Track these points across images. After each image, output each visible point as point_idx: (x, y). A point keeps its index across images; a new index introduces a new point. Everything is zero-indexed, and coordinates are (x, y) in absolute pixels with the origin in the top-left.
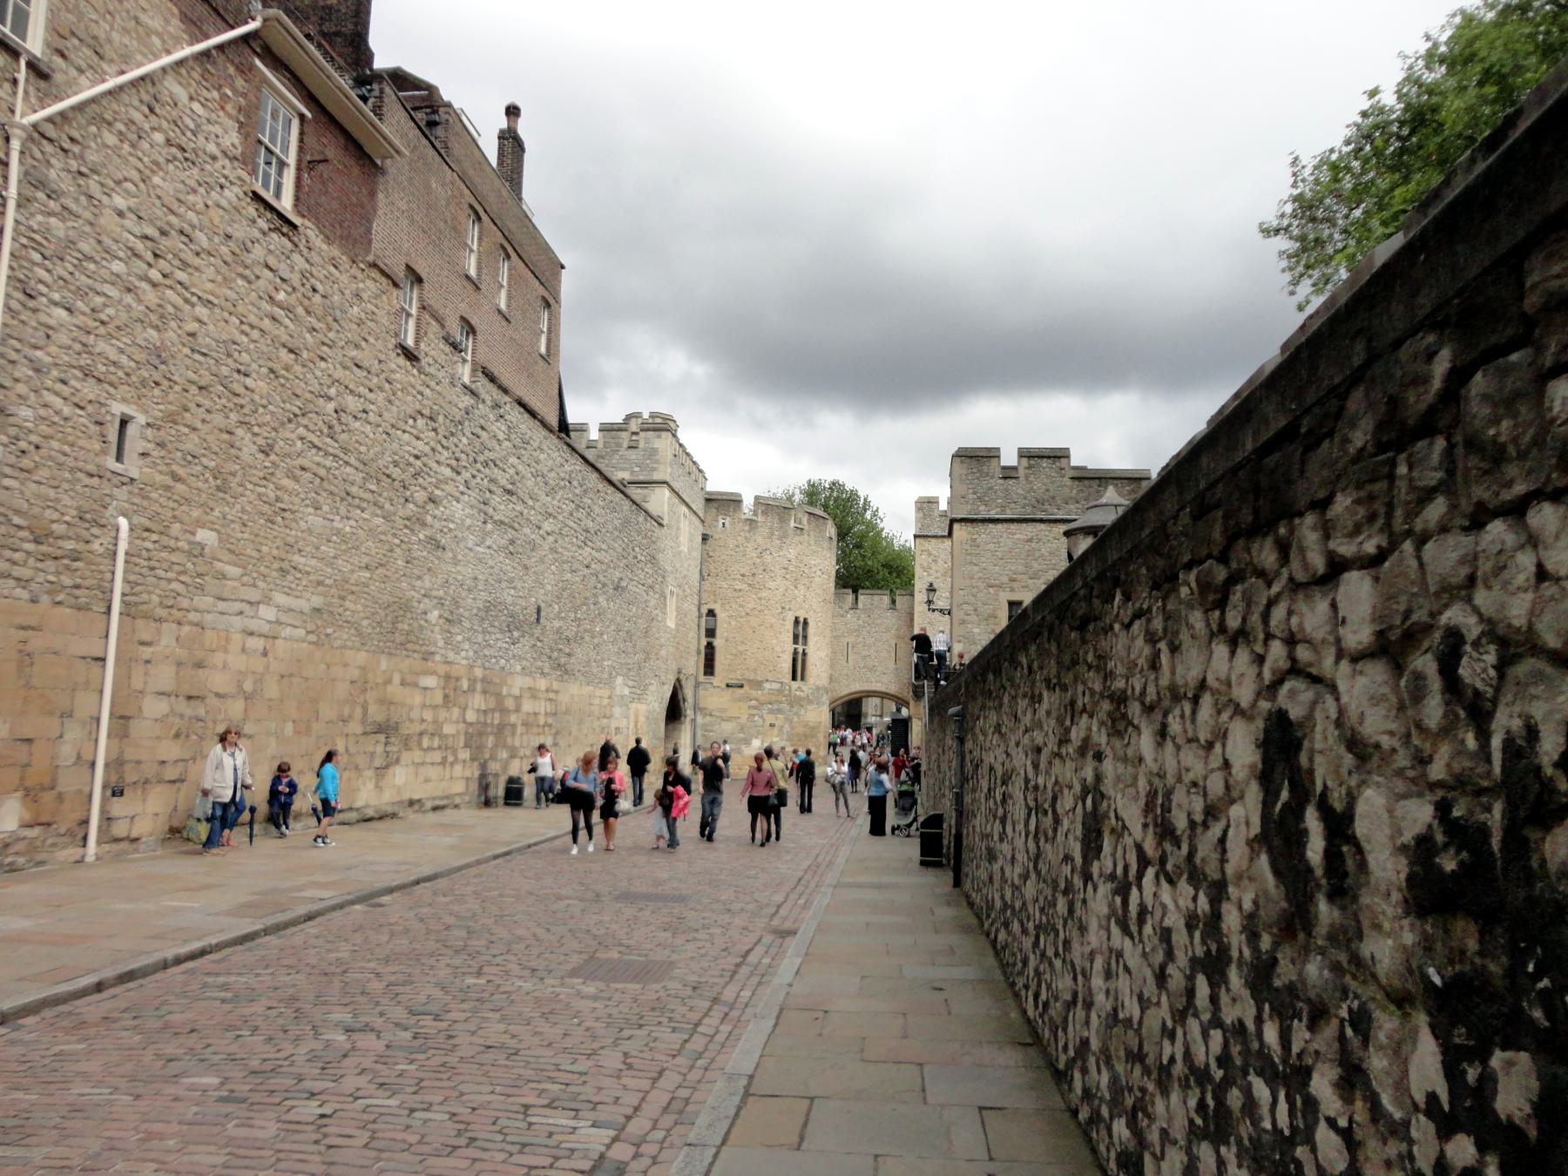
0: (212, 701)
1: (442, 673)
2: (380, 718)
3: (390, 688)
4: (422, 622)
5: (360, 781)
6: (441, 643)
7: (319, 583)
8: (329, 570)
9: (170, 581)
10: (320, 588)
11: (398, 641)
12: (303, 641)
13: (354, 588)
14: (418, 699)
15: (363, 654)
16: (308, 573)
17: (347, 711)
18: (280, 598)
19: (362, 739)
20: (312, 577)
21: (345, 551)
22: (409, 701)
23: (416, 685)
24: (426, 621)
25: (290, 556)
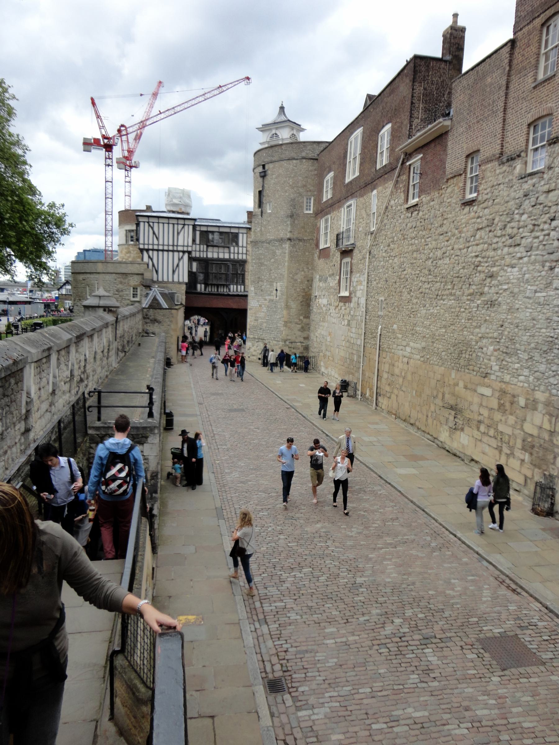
0: (396, 376)
1: (498, 389)
2: (452, 402)
3: (457, 388)
4: (479, 354)
5: (441, 429)
6: (497, 368)
7: (424, 337)
8: (428, 331)
9: (389, 341)
10: (425, 339)
11: (462, 364)
12: (419, 360)
13: (437, 337)
14: (476, 400)
15: (443, 368)
16: (420, 334)
17: (435, 394)
18: (412, 344)
19: (442, 408)
20: (422, 335)
21: (434, 322)
22: (470, 399)
23: (475, 391)
24: (483, 353)
25: (415, 328)
